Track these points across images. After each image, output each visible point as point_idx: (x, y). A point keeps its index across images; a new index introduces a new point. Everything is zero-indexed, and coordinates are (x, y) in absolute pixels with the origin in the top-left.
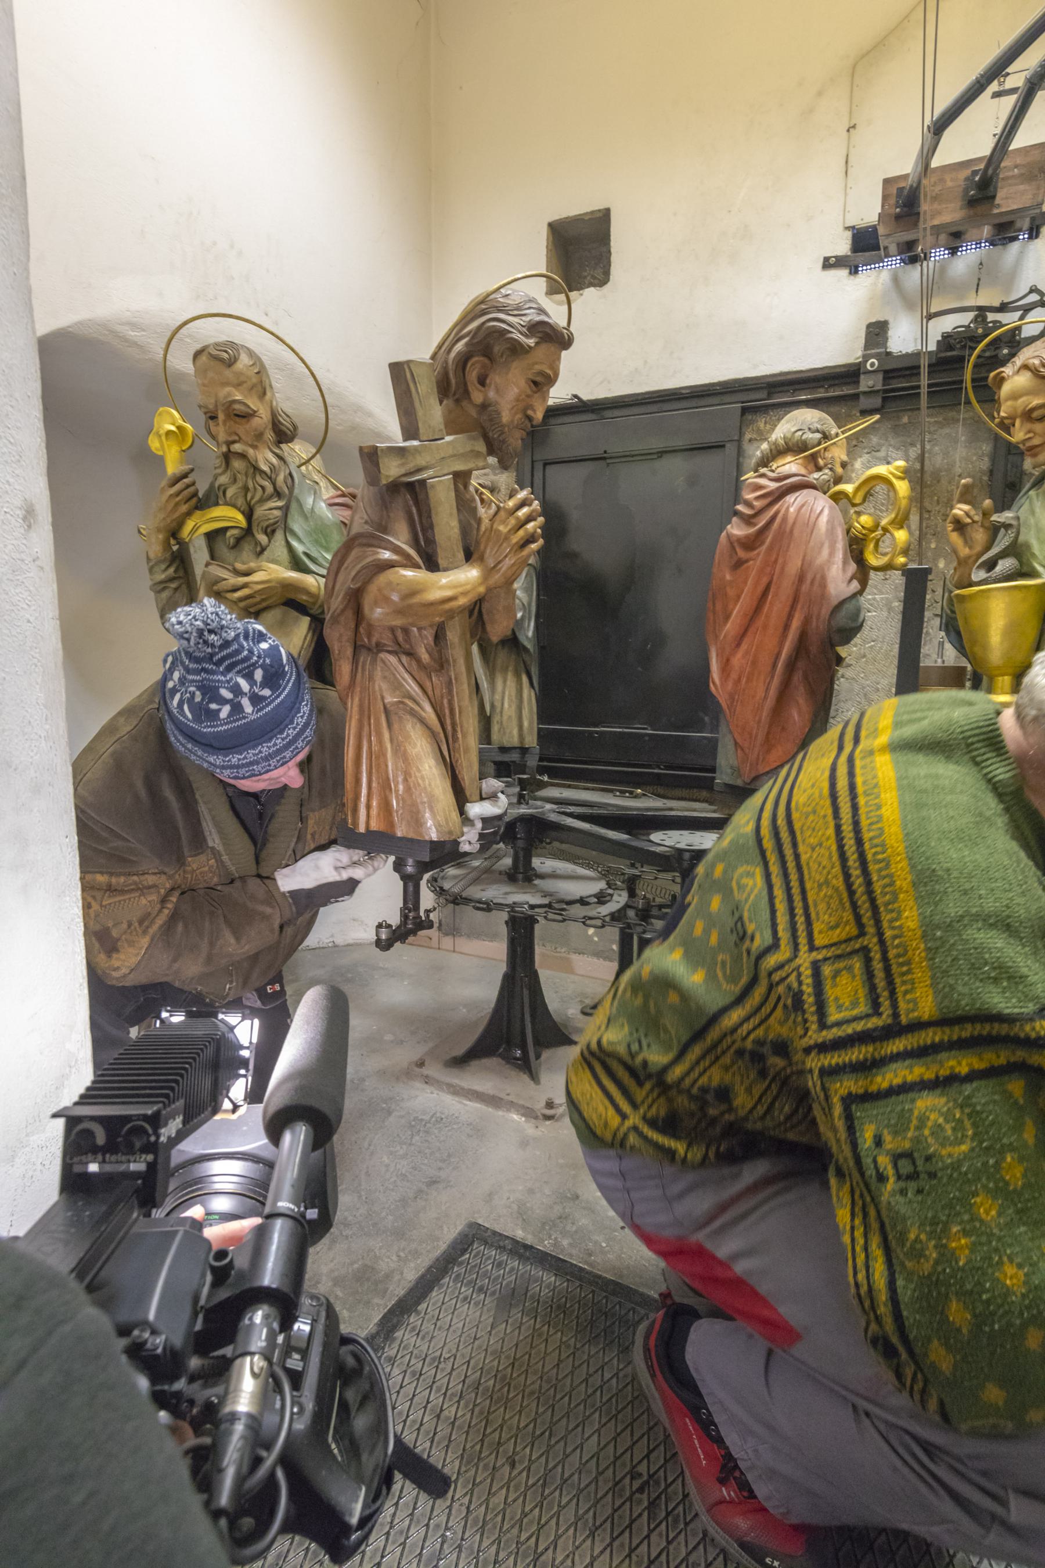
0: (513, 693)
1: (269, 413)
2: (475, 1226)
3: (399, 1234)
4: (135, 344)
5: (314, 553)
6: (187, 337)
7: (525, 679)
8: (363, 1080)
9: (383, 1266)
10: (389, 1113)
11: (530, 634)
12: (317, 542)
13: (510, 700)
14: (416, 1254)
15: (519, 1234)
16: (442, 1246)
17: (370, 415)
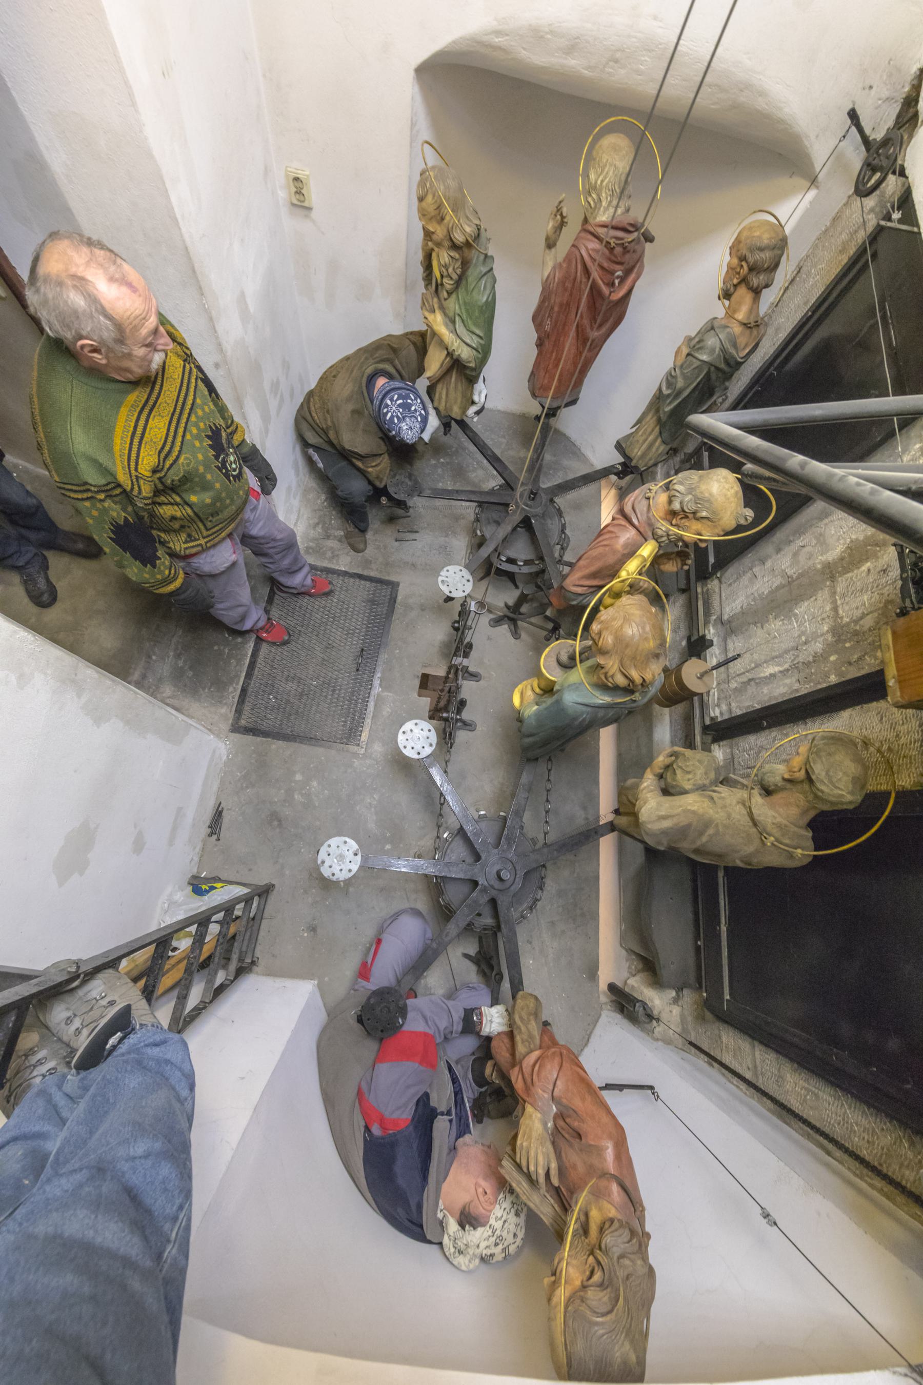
0: (649, 430)
1: (445, 231)
2: (398, 584)
3: (387, 564)
4: (499, 48)
5: (464, 317)
6: (547, 33)
7: (657, 429)
8: (463, 518)
9: (373, 566)
10: (446, 536)
11: (668, 409)
12: (467, 310)
13: (644, 433)
14: (381, 572)
15: (399, 598)
16: (387, 578)
17: (762, 94)
